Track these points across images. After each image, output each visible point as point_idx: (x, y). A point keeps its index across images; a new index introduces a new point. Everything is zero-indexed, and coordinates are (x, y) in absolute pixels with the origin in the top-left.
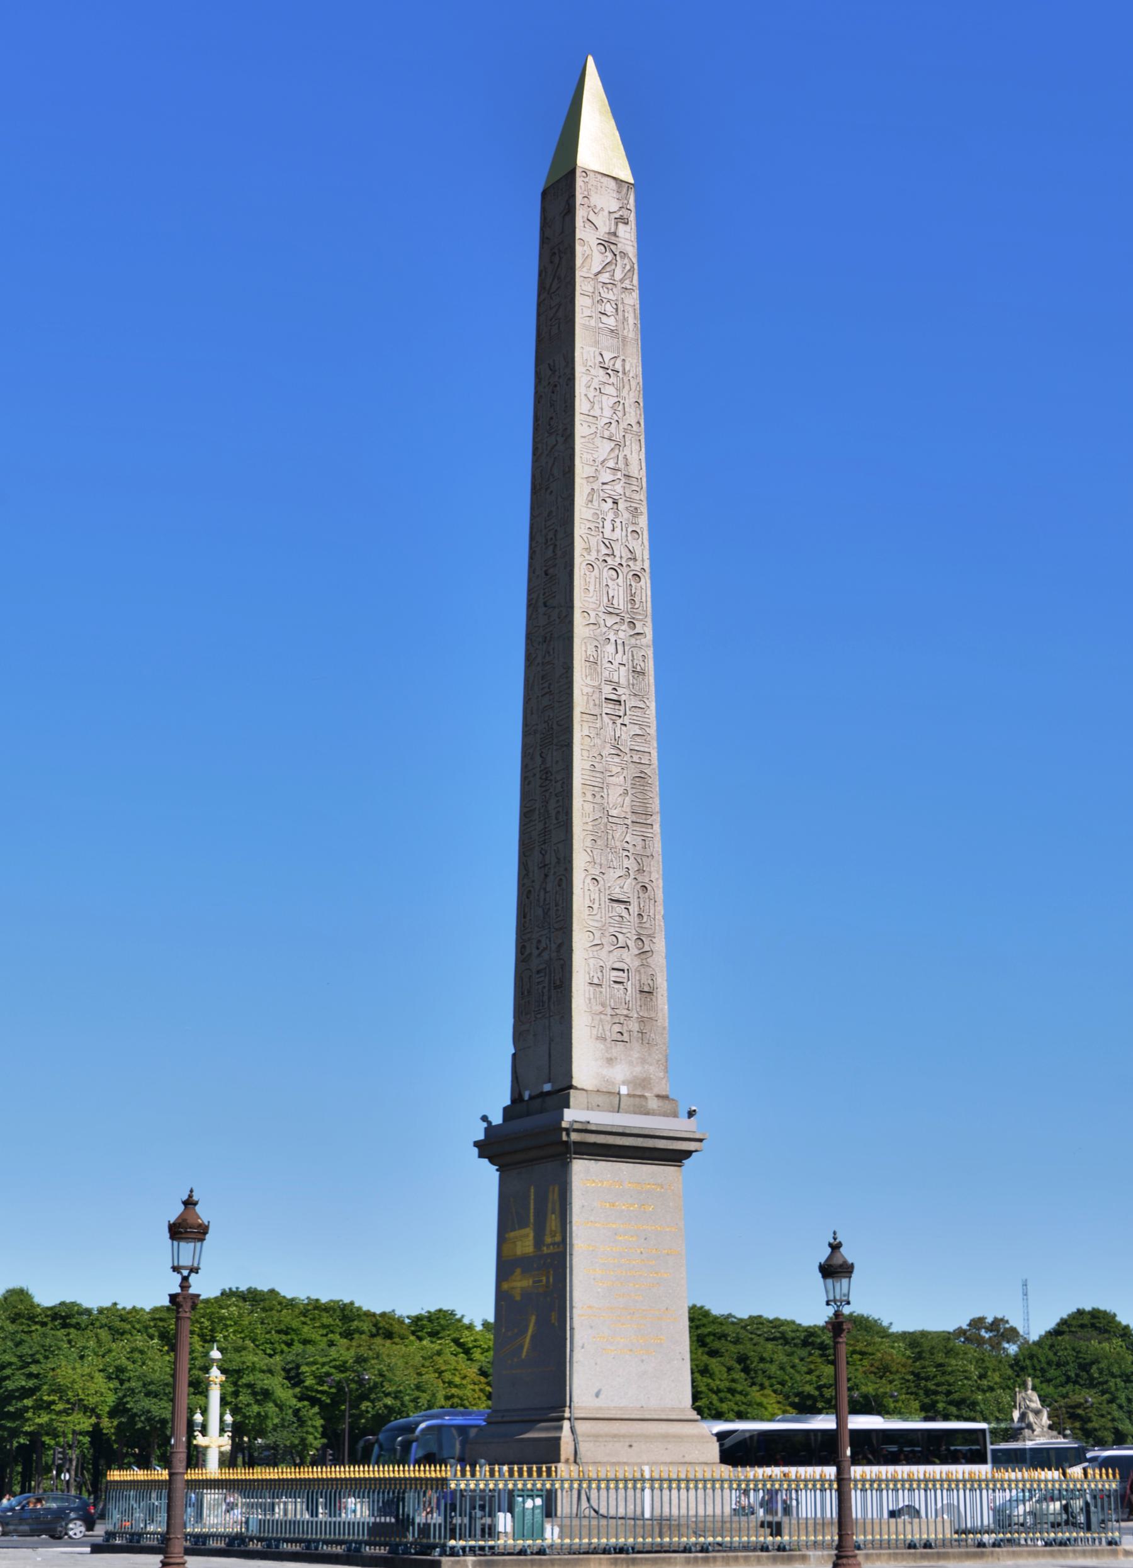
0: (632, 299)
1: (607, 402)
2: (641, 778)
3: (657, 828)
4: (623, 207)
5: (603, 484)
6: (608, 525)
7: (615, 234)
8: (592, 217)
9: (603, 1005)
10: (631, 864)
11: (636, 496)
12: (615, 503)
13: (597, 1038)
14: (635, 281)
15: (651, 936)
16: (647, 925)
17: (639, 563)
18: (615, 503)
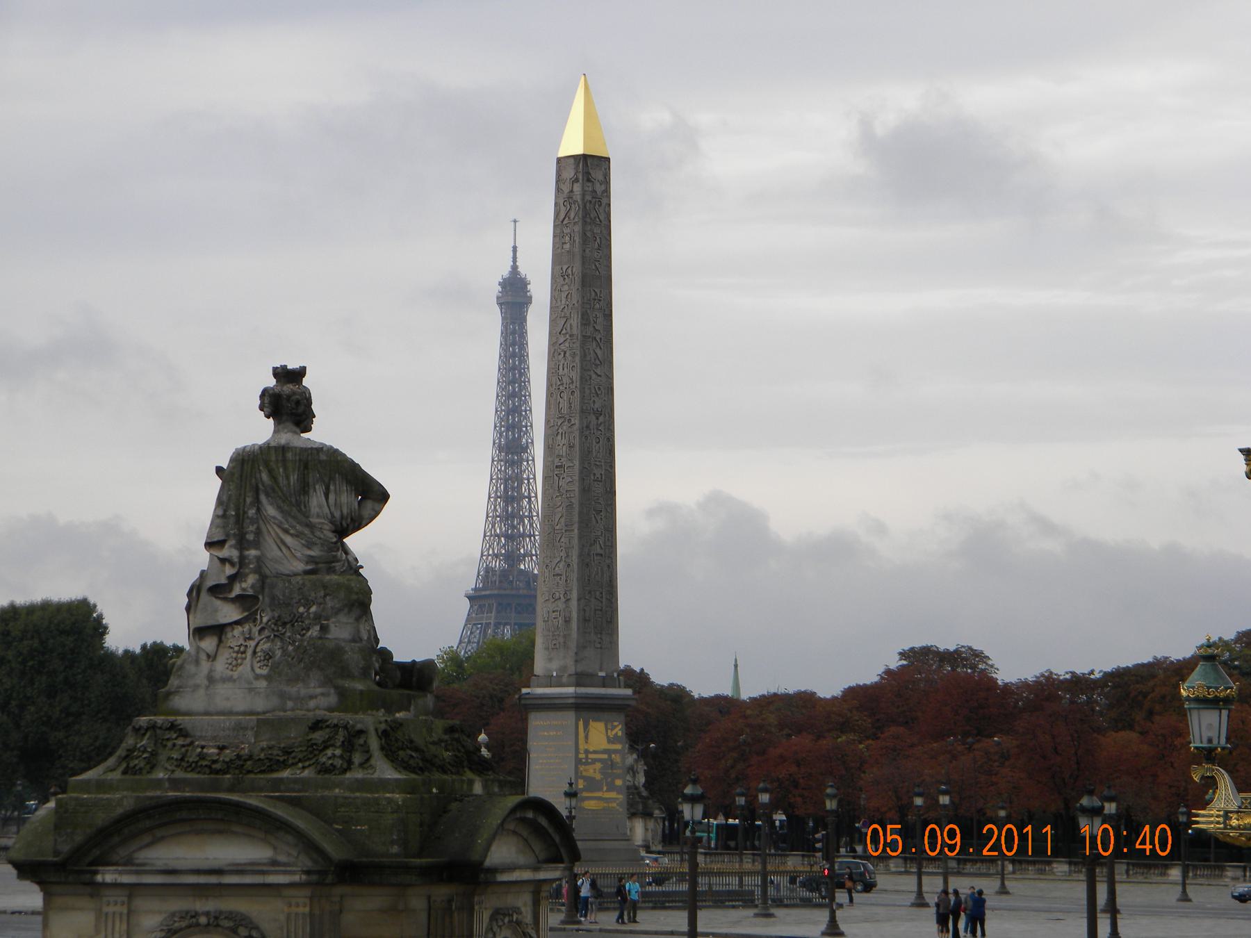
0: (577, 228)
1: (564, 295)
2: (570, 506)
3: (576, 531)
4: (577, 172)
5: (560, 344)
6: (561, 367)
7: (572, 191)
8: (562, 186)
9: (549, 630)
10: (563, 554)
11: (574, 346)
12: (565, 353)
13: (545, 649)
14: (580, 216)
15: (571, 590)
16: (569, 585)
17: (574, 384)
18: (565, 353)
